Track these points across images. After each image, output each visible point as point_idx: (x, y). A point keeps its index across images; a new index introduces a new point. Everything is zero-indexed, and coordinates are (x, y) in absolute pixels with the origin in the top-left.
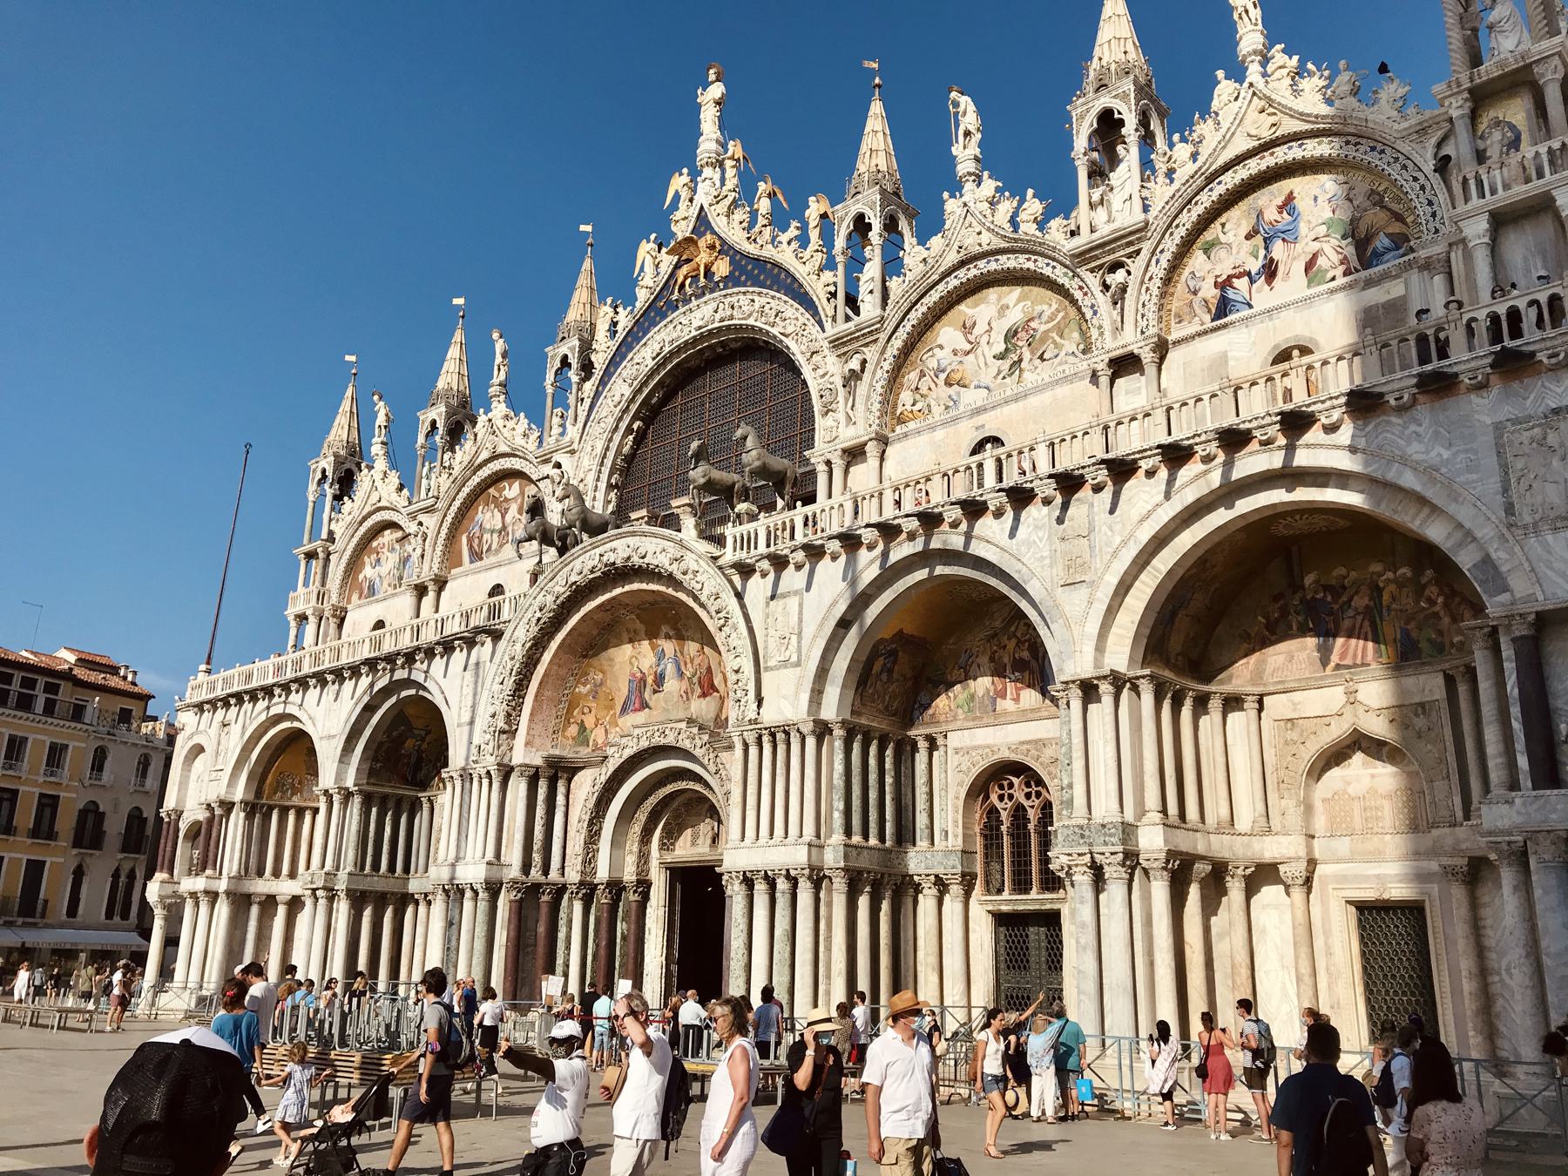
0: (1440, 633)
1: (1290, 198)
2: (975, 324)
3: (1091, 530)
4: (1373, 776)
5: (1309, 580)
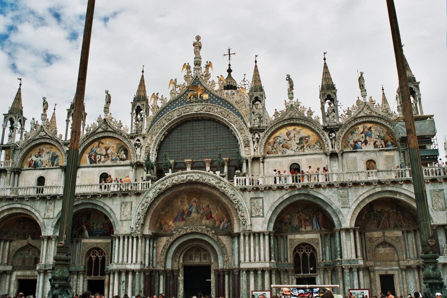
0: (401, 223)
1: (370, 128)
2: (290, 134)
3: (348, 195)
4: (384, 250)
5: (375, 209)
